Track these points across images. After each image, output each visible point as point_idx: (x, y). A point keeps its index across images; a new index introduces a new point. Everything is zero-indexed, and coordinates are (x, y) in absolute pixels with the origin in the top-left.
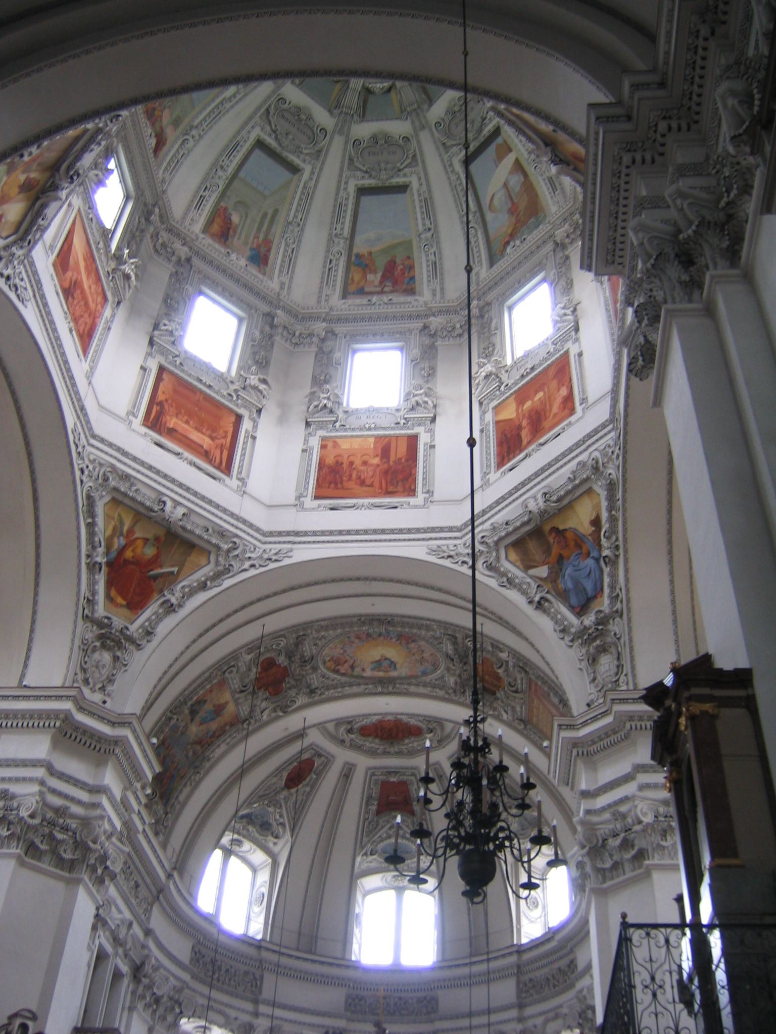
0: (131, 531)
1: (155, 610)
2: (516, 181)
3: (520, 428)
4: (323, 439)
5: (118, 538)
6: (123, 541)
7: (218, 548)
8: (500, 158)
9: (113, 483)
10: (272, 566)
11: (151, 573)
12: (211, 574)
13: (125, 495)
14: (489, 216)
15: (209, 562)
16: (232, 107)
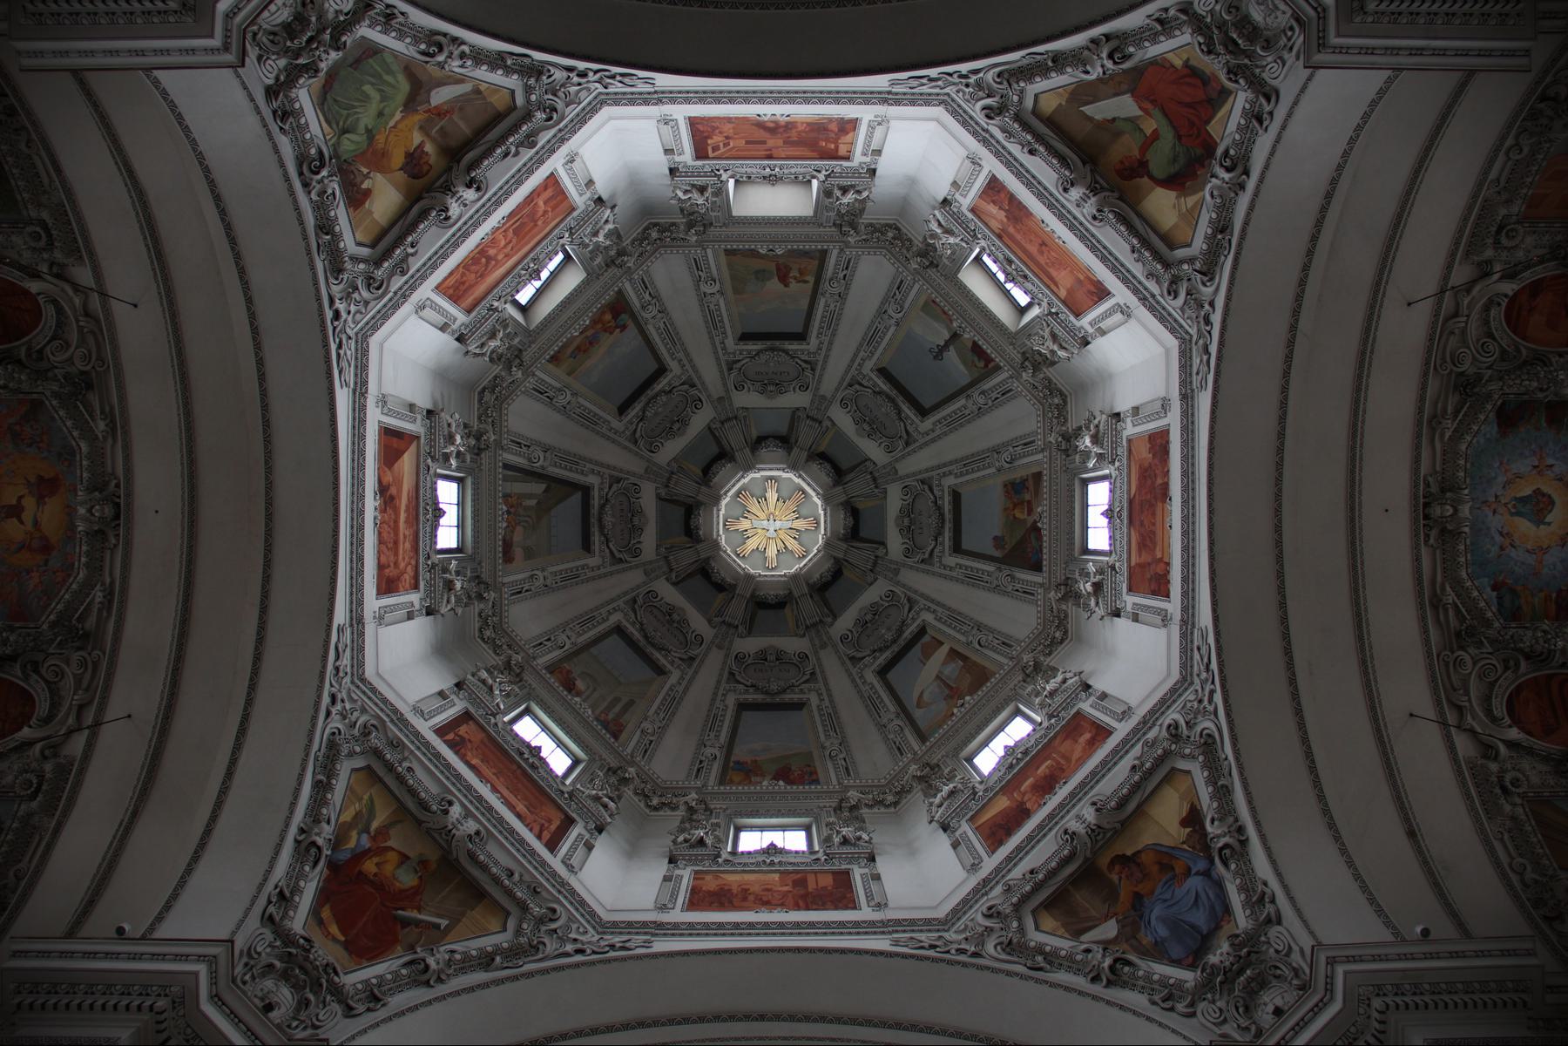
0: (383, 832)
1: (394, 968)
2: (953, 670)
3: (1022, 803)
4: (696, 872)
5: (359, 834)
6: (366, 842)
7: (523, 907)
8: (927, 654)
9: (375, 740)
10: (612, 954)
11: (400, 912)
12: (505, 945)
13: (390, 768)
14: (918, 714)
15: (505, 929)
16: (594, 579)
